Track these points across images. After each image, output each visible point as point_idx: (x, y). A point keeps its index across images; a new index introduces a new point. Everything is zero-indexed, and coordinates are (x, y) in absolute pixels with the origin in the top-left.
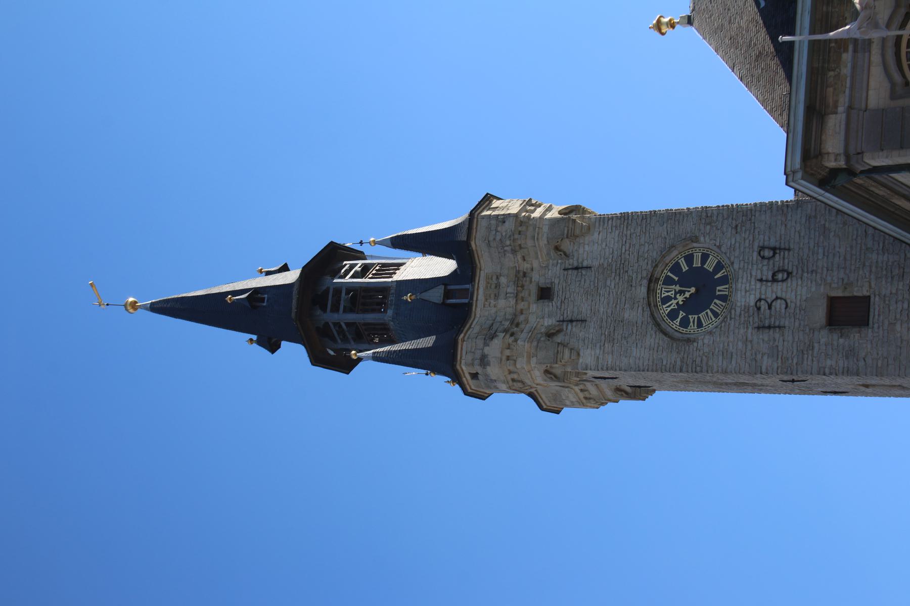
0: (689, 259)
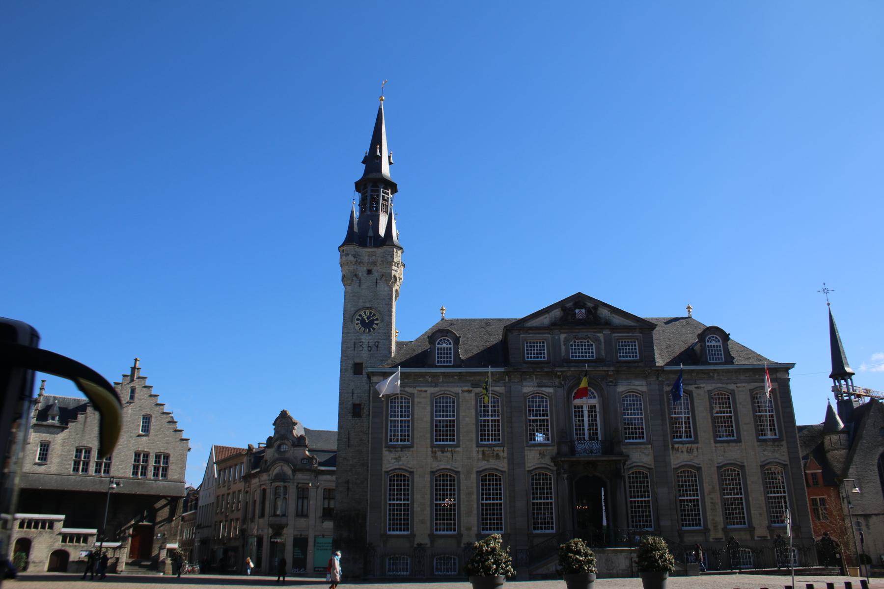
0: (377, 319)
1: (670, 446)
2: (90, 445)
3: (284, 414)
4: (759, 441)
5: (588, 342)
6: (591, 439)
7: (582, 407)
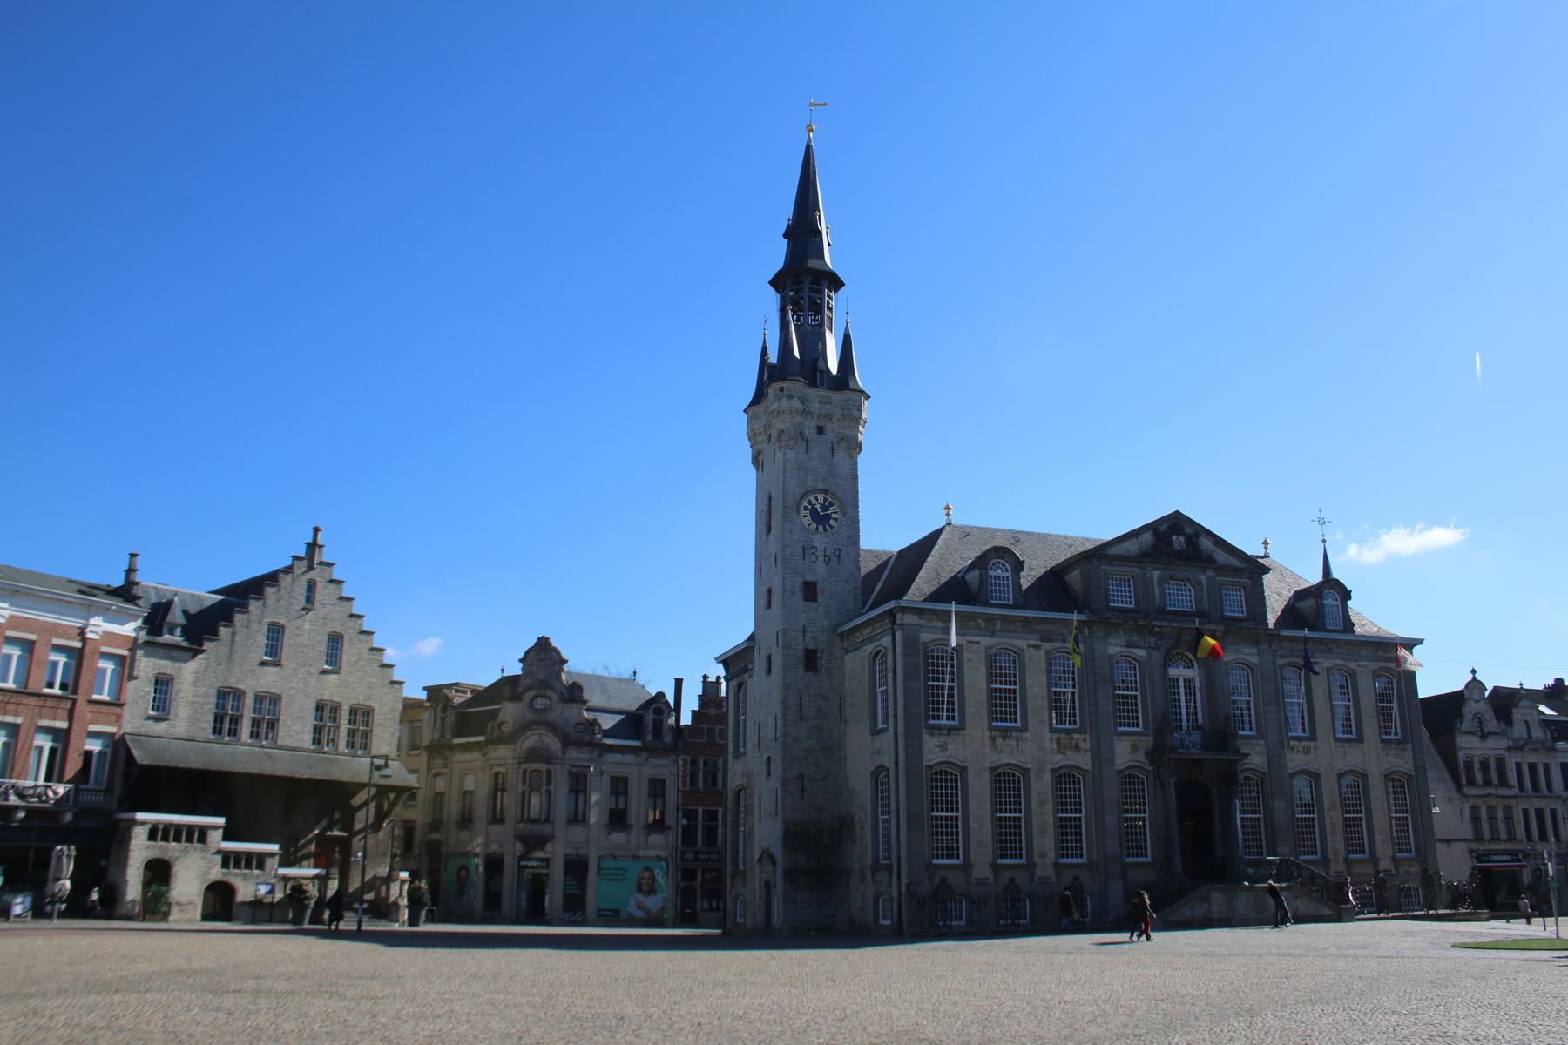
1: (1286, 743)
2: (242, 687)
3: (543, 645)
4: (1383, 741)
5: (1185, 585)
7: (1178, 679)
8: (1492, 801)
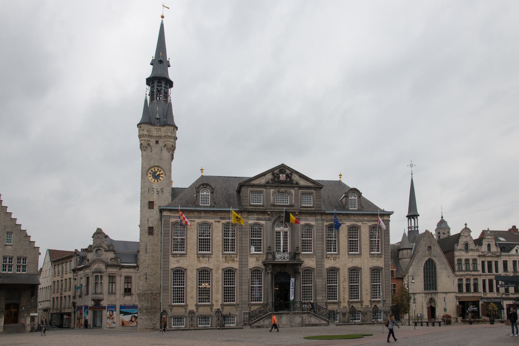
1: (325, 256)
6: (284, 251)
8: (468, 277)
